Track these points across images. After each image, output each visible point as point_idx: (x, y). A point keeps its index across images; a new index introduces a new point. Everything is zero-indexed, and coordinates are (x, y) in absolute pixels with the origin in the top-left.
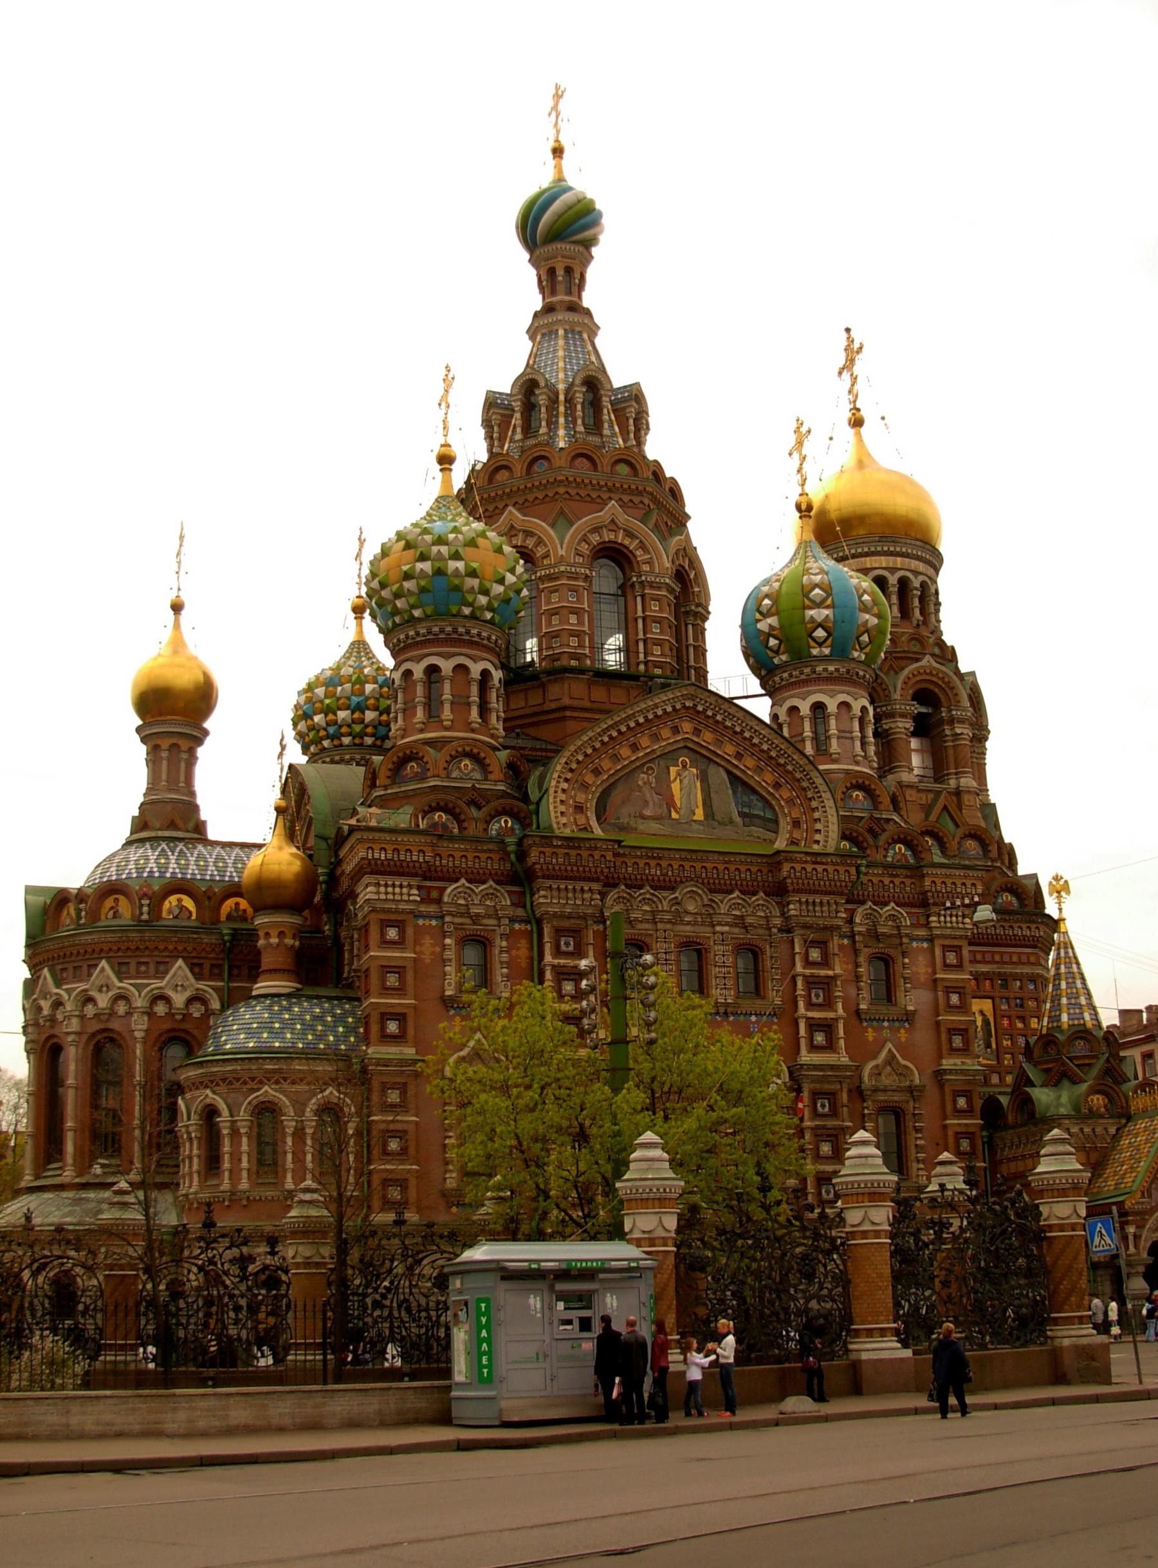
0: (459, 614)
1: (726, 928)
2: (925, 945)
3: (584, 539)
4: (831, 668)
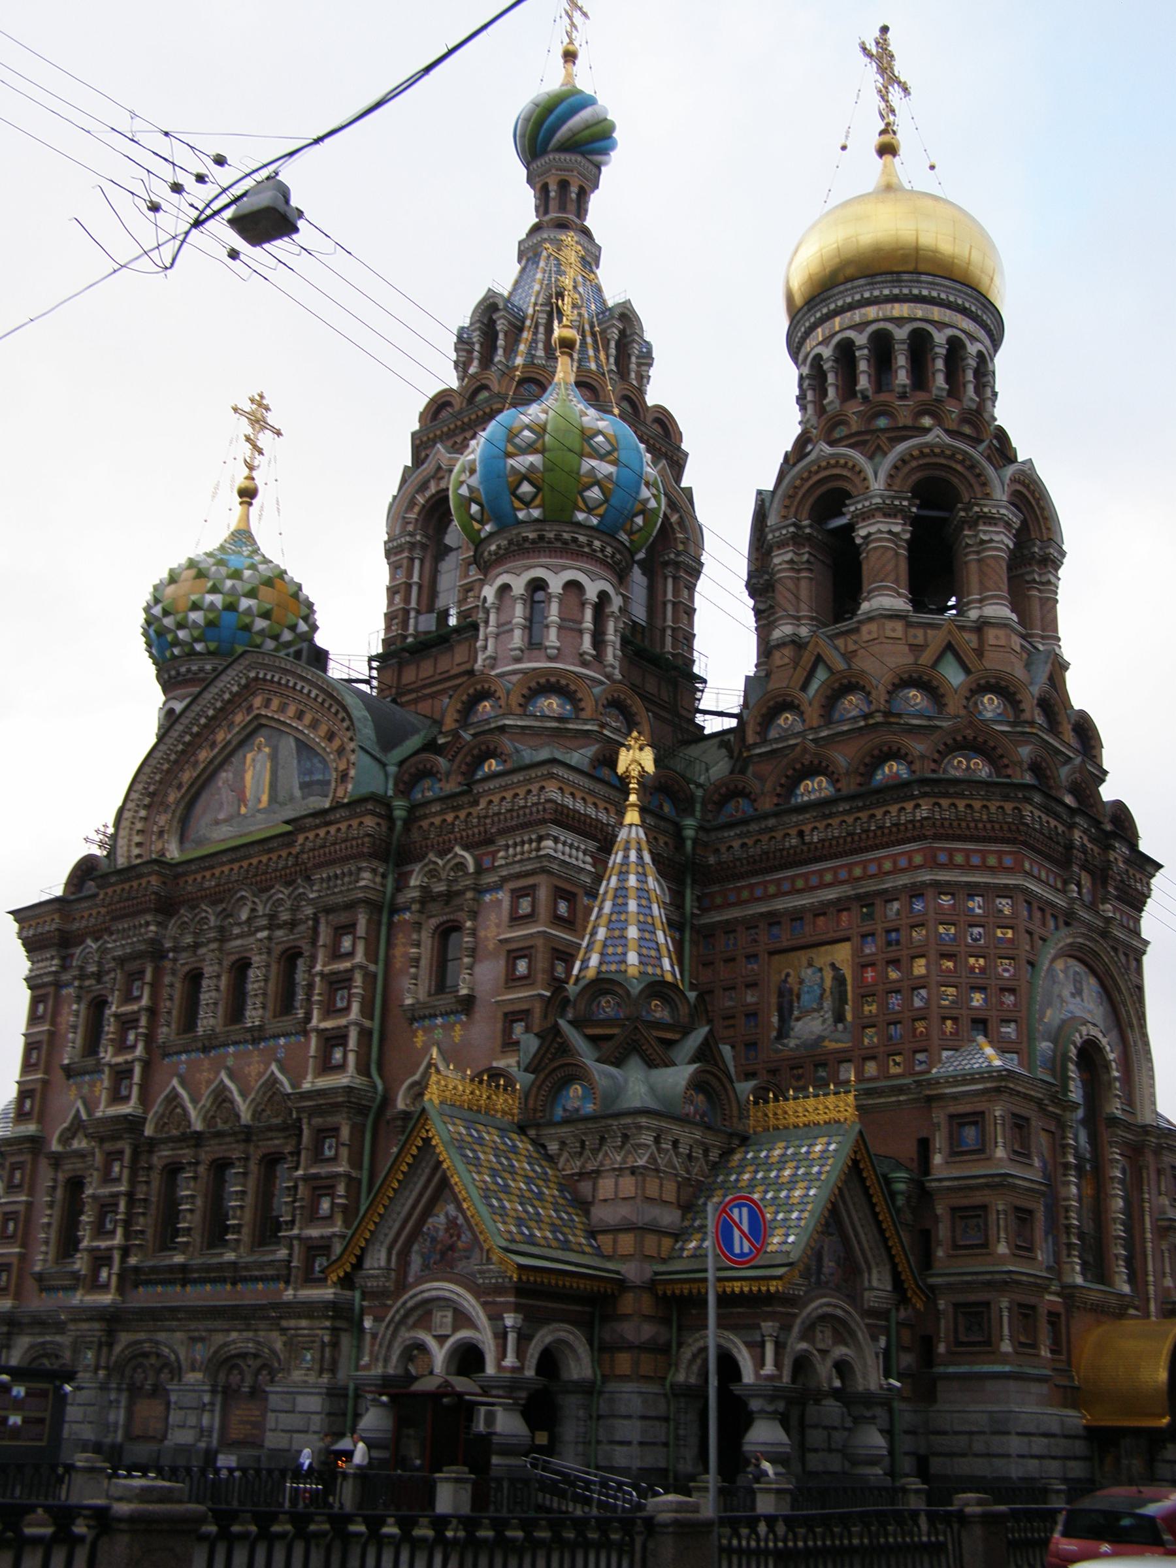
0: (174, 657)
1: (265, 934)
2: (500, 895)
3: (412, 503)
4: (493, 548)
